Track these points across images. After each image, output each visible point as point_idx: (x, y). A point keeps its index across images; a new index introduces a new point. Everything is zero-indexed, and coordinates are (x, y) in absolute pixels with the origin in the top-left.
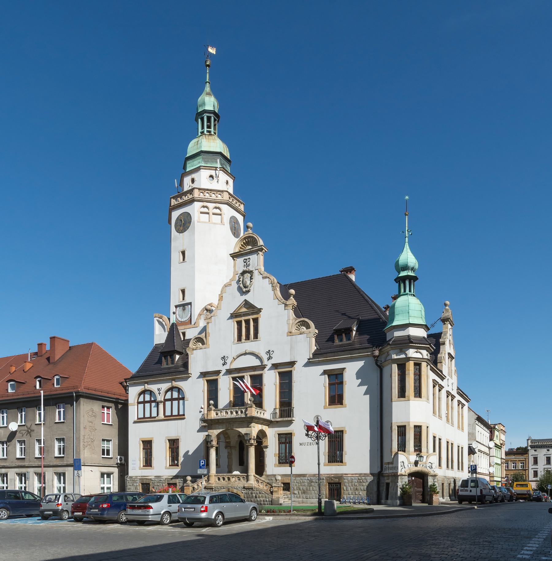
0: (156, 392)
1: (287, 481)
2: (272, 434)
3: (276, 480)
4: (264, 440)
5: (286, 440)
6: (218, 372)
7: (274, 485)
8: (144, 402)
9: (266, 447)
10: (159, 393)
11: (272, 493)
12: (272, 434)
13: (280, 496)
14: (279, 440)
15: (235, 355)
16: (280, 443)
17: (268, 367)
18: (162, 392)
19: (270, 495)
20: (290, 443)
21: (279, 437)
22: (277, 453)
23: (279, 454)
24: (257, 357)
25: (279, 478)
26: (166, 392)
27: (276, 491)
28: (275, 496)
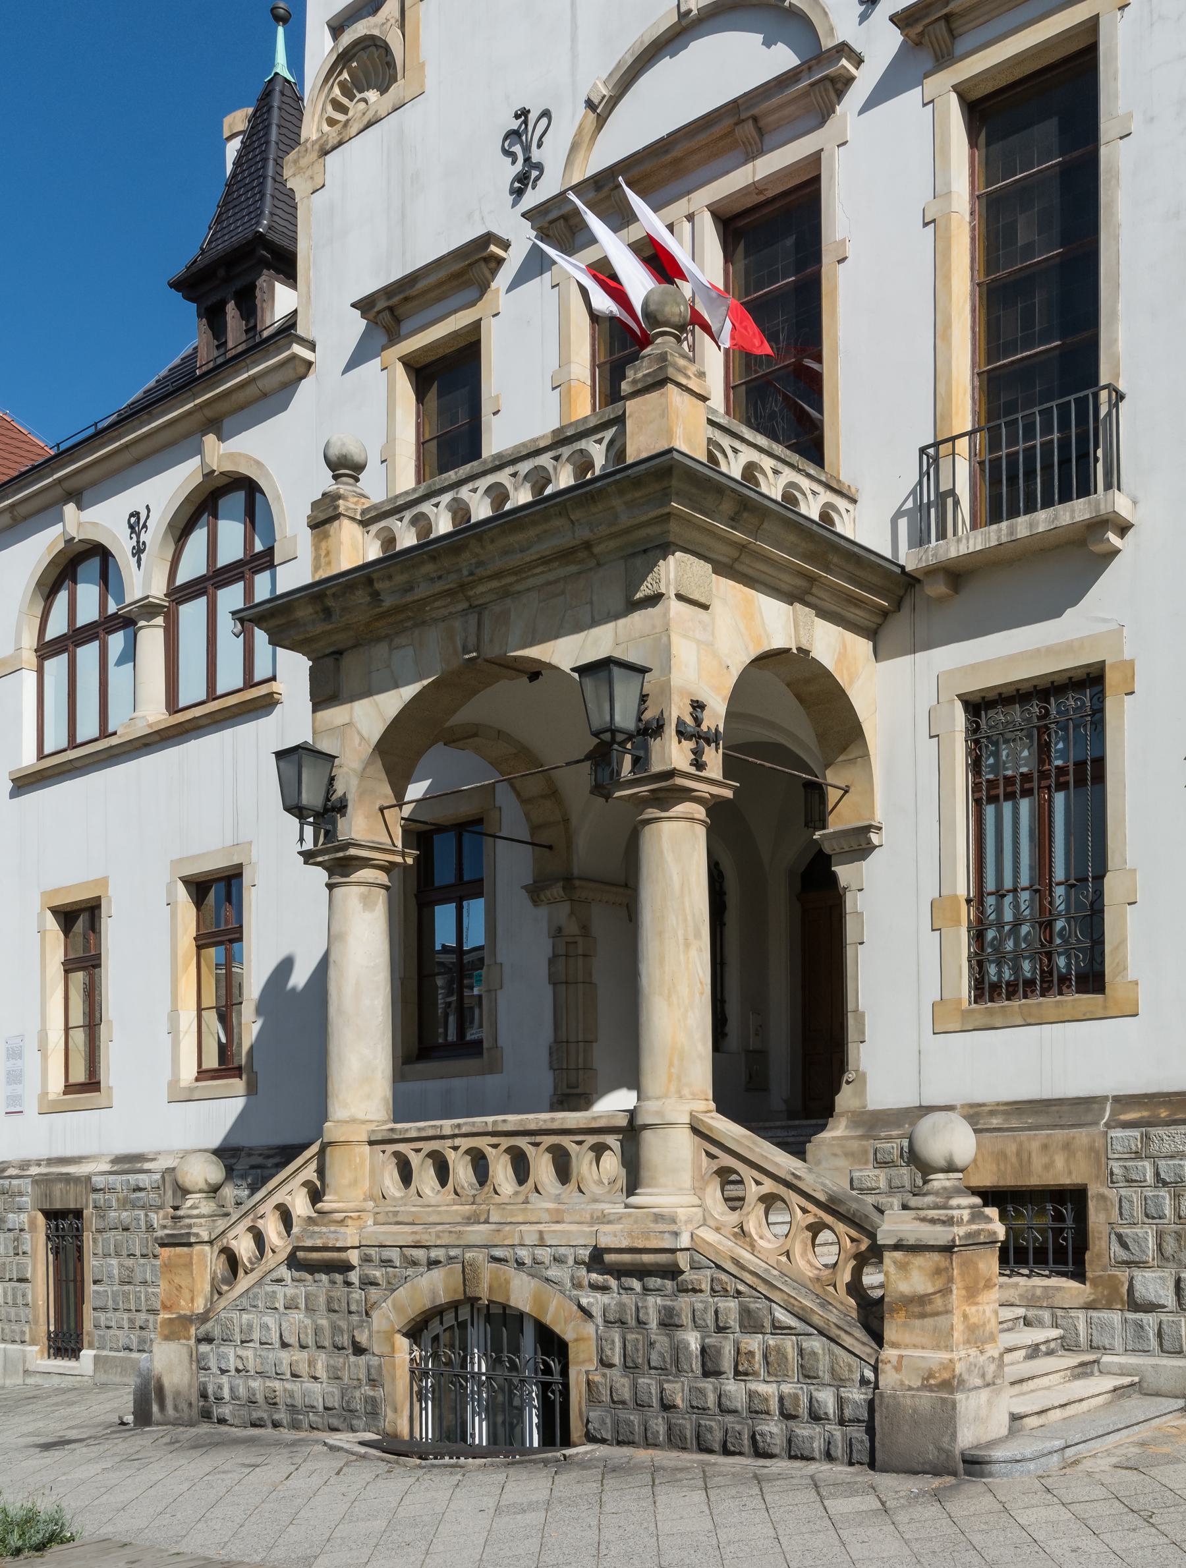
1: (1058, 1171)
2: (906, 714)
3: (925, 1168)
4: (833, 777)
5: (1044, 750)
7: (896, 1225)
8: (77, 637)
9: (860, 843)
11: (872, 1315)
12: (906, 714)
13: (963, 1358)
14: (975, 765)
15: (596, 78)
16: (988, 791)
17: (866, 80)
19: (857, 1339)
20: (1090, 775)
21: (973, 730)
22: (962, 886)
23: (978, 900)
25: (953, 1141)
26: (181, 529)
27: (918, 1305)
28: (908, 1355)
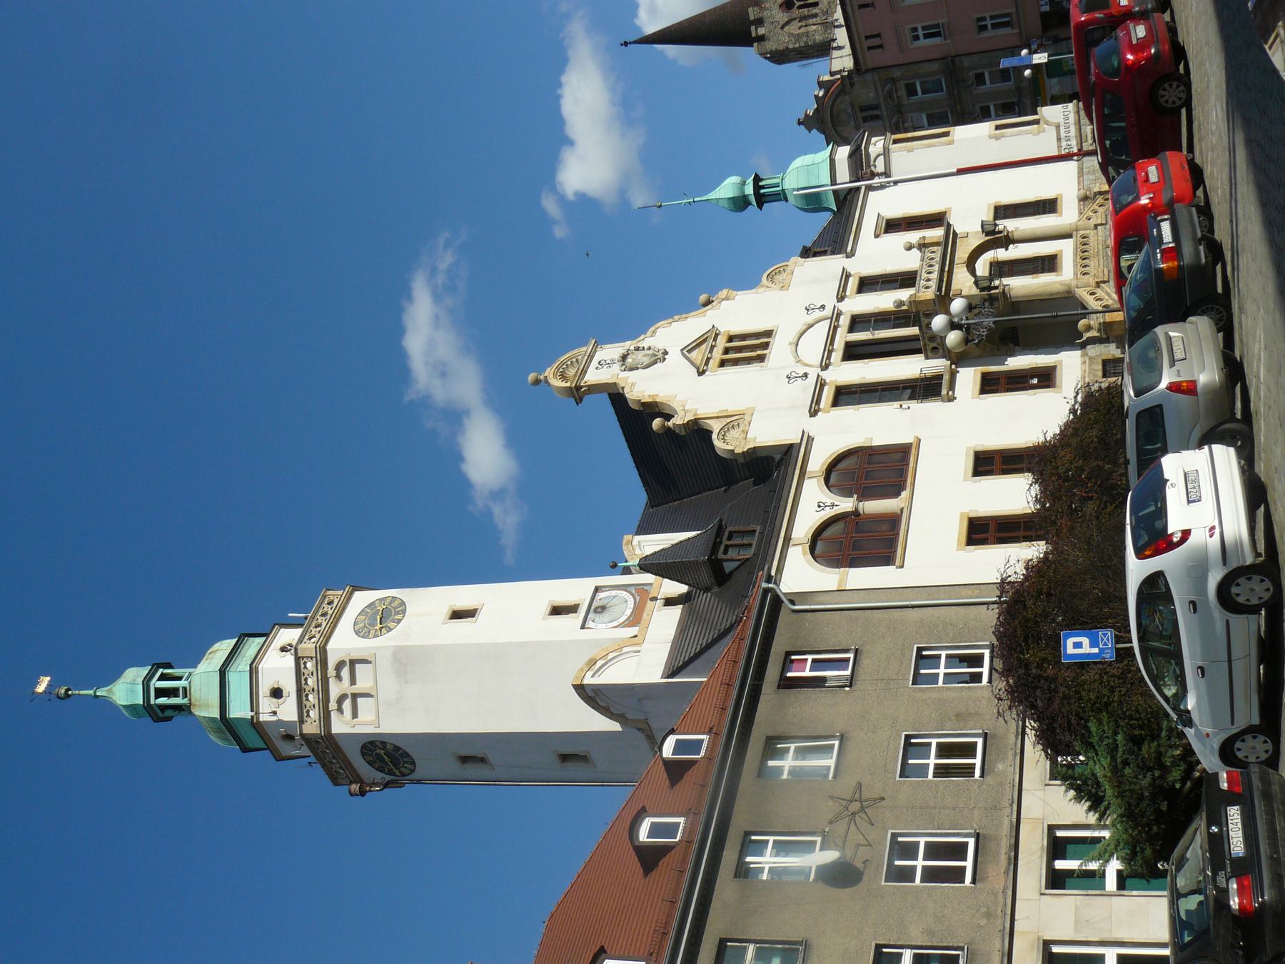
0: (828, 513)
6: (821, 385)
10: (833, 505)
18: (828, 497)
24: (811, 326)
